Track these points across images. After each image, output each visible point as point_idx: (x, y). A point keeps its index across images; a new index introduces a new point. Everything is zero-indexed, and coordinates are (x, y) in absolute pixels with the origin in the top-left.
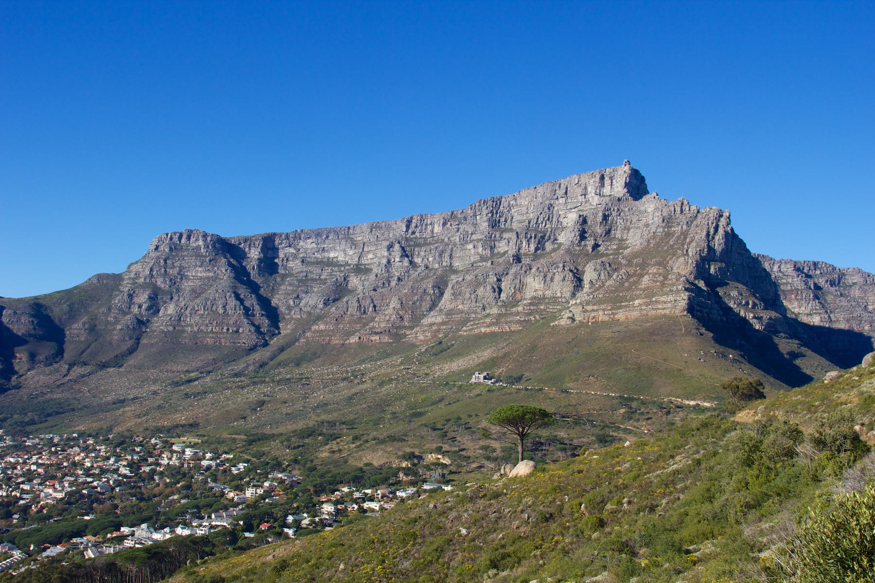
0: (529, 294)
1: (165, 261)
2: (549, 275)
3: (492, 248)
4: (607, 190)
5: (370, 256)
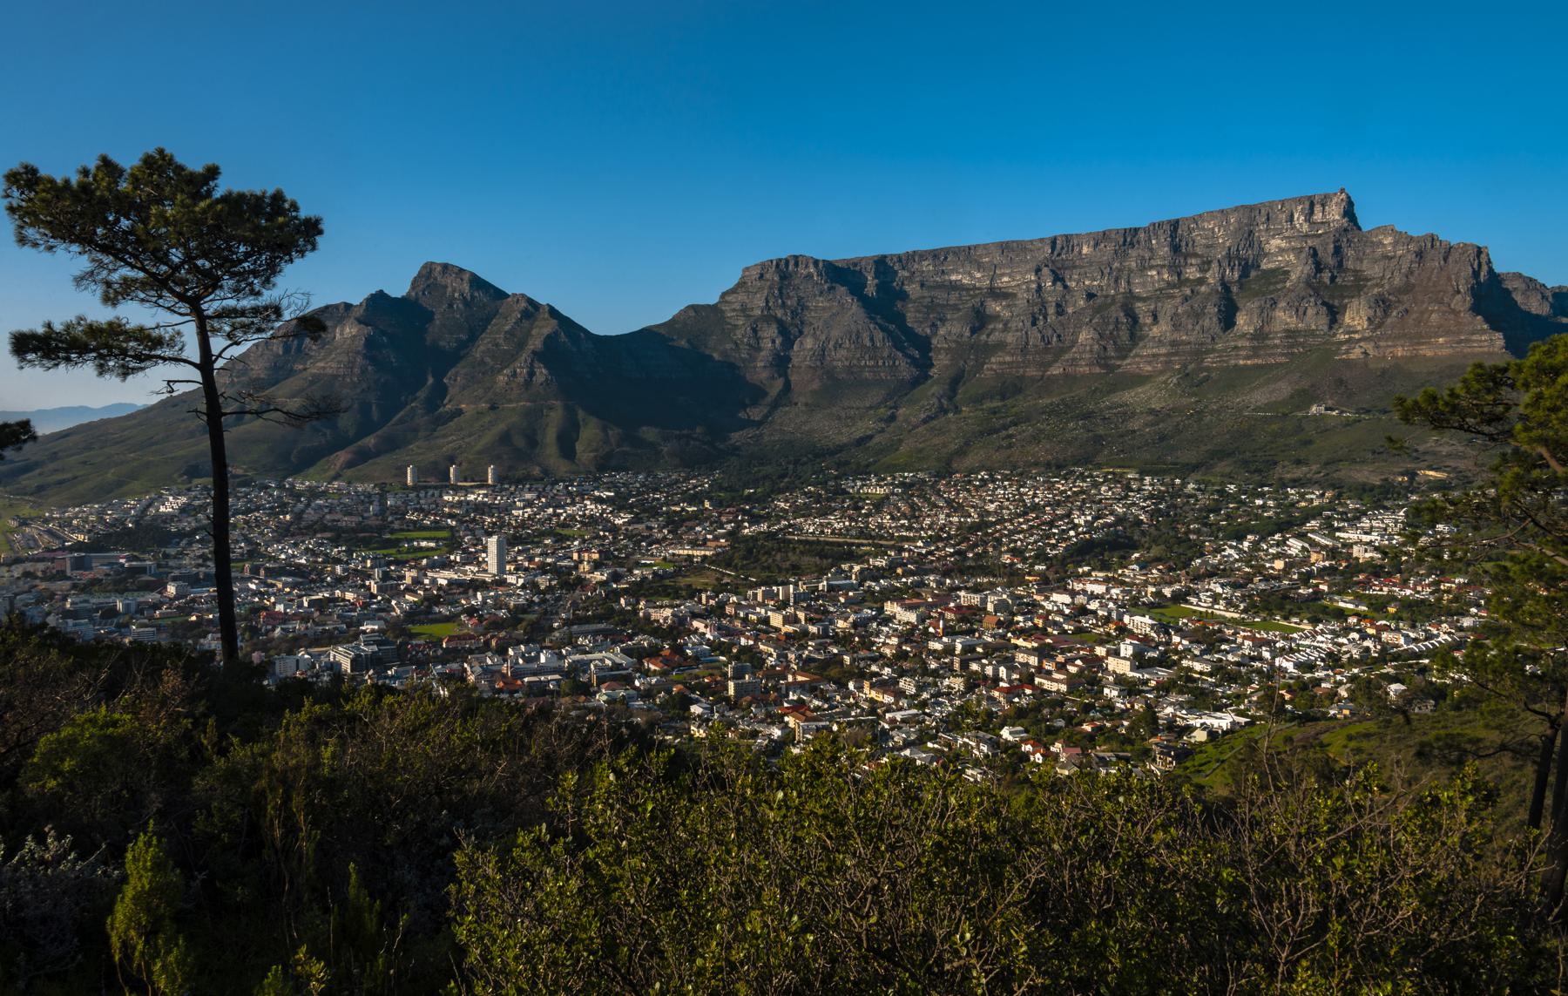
0: (1277, 327)
1: (780, 290)
2: (1301, 310)
3: (1179, 275)
4: (1318, 216)
5: (1006, 279)
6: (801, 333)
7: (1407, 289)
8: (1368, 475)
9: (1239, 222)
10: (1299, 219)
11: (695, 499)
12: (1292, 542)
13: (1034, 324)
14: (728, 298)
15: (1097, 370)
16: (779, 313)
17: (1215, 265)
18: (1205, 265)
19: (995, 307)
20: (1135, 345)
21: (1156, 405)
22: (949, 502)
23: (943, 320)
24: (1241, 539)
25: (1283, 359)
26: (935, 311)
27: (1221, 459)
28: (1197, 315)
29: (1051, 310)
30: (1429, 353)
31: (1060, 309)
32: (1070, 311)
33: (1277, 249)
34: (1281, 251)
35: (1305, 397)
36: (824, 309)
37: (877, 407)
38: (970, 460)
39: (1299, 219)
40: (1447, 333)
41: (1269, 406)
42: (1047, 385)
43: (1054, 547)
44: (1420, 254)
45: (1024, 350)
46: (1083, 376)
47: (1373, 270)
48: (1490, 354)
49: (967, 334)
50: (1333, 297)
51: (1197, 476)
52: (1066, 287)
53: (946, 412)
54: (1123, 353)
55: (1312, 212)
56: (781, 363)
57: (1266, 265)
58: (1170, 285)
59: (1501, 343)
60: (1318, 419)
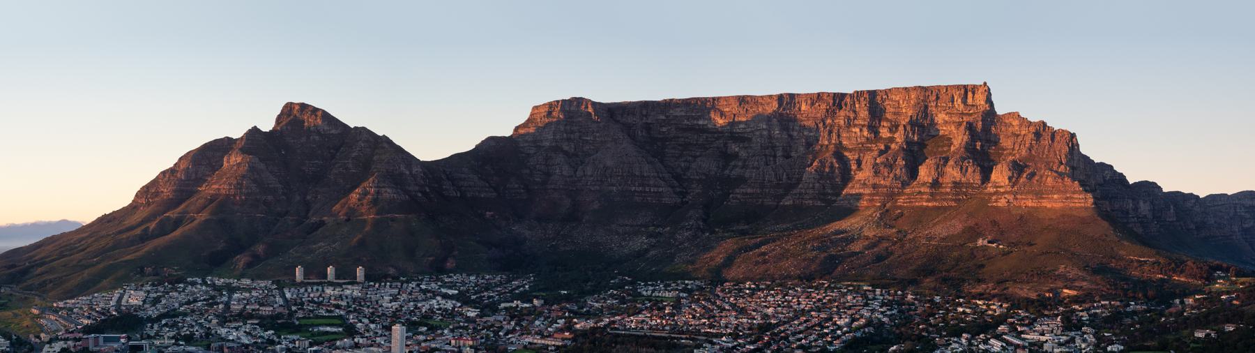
4: (970, 101)
7: (1030, 157)
10: (958, 101)
11: (525, 297)
12: (992, 341)
15: (819, 203)
17: (901, 128)
18: (894, 128)
19: (734, 148)
22: (733, 306)
24: (959, 336)
27: (925, 276)
28: (890, 166)
29: (779, 153)
30: (1049, 206)
31: (788, 157)
32: (793, 154)
35: (973, 232)
38: (734, 272)
40: (1059, 192)
43: (830, 343)
48: (1086, 208)
51: (912, 288)
52: (790, 136)
59: (1091, 201)
60: (984, 248)
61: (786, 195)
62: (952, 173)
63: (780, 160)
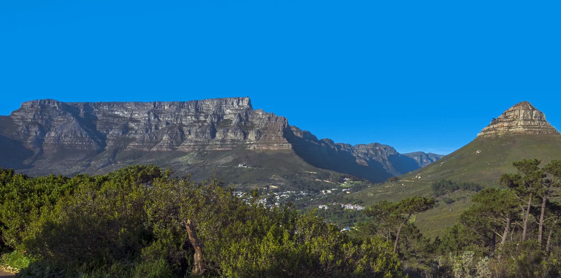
0: (229, 138)
1: (41, 112)
4: (241, 104)
5: (136, 115)
6: (49, 130)
7: (266, 129)
8: (254, 187)
9: (217, 103)
10: (235, 104)
13: (147, 132)
14: (15, 114)
15: (169, 150)
16: (40, 122)
17: (209, 116)
18: (206, 116)
19: (132, 125)
20: (183, 141)
21: (190, 163)
23: (111, 129)
25: (230, 149)
26: (109, 126)
28: (203, 133)
29: (153, 128)
30: (272, 149)
31: (157, 128)
32: (160, 128)
33: (229, 113)
34: (230, 114)
35: (237, 162)
36: (60, 121)
37: (83, 160)
39: (235, 104)
40: (277, 143)
41: (226, 164)
42: (151, 155)
44: (269, 118)
45: (143, 141)
46: (164, 152)
47: (256, 122)
48: (288, 150)
49: (121, 134)
50: (245, 130)
52: (159, 120)
53: (111, 163)
54: (179, 144)
55: (239, 102)
56: (39, 141)
57: (225, 118)
58: (195, 122)
59: (291, 147)
60: (242, 168)
61: (154, 146)
62: (231, 135)
63: (153, 130)
